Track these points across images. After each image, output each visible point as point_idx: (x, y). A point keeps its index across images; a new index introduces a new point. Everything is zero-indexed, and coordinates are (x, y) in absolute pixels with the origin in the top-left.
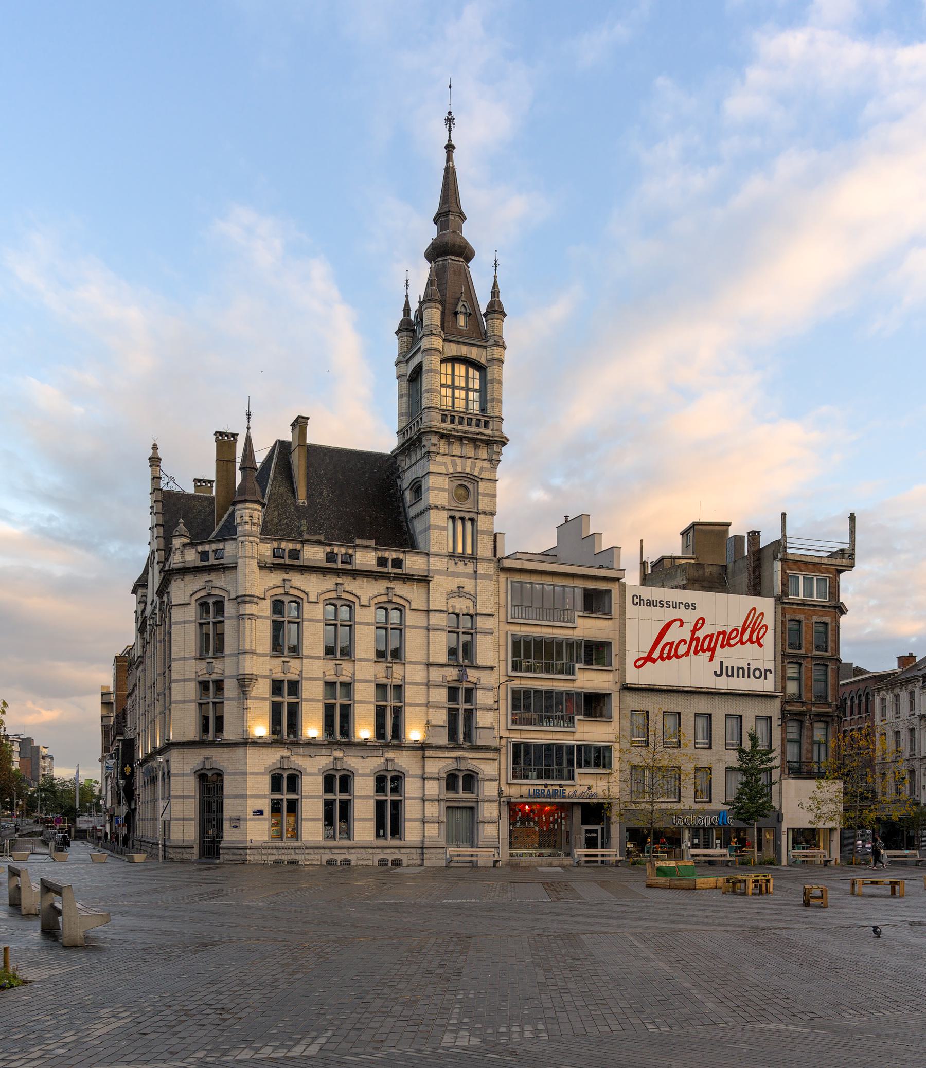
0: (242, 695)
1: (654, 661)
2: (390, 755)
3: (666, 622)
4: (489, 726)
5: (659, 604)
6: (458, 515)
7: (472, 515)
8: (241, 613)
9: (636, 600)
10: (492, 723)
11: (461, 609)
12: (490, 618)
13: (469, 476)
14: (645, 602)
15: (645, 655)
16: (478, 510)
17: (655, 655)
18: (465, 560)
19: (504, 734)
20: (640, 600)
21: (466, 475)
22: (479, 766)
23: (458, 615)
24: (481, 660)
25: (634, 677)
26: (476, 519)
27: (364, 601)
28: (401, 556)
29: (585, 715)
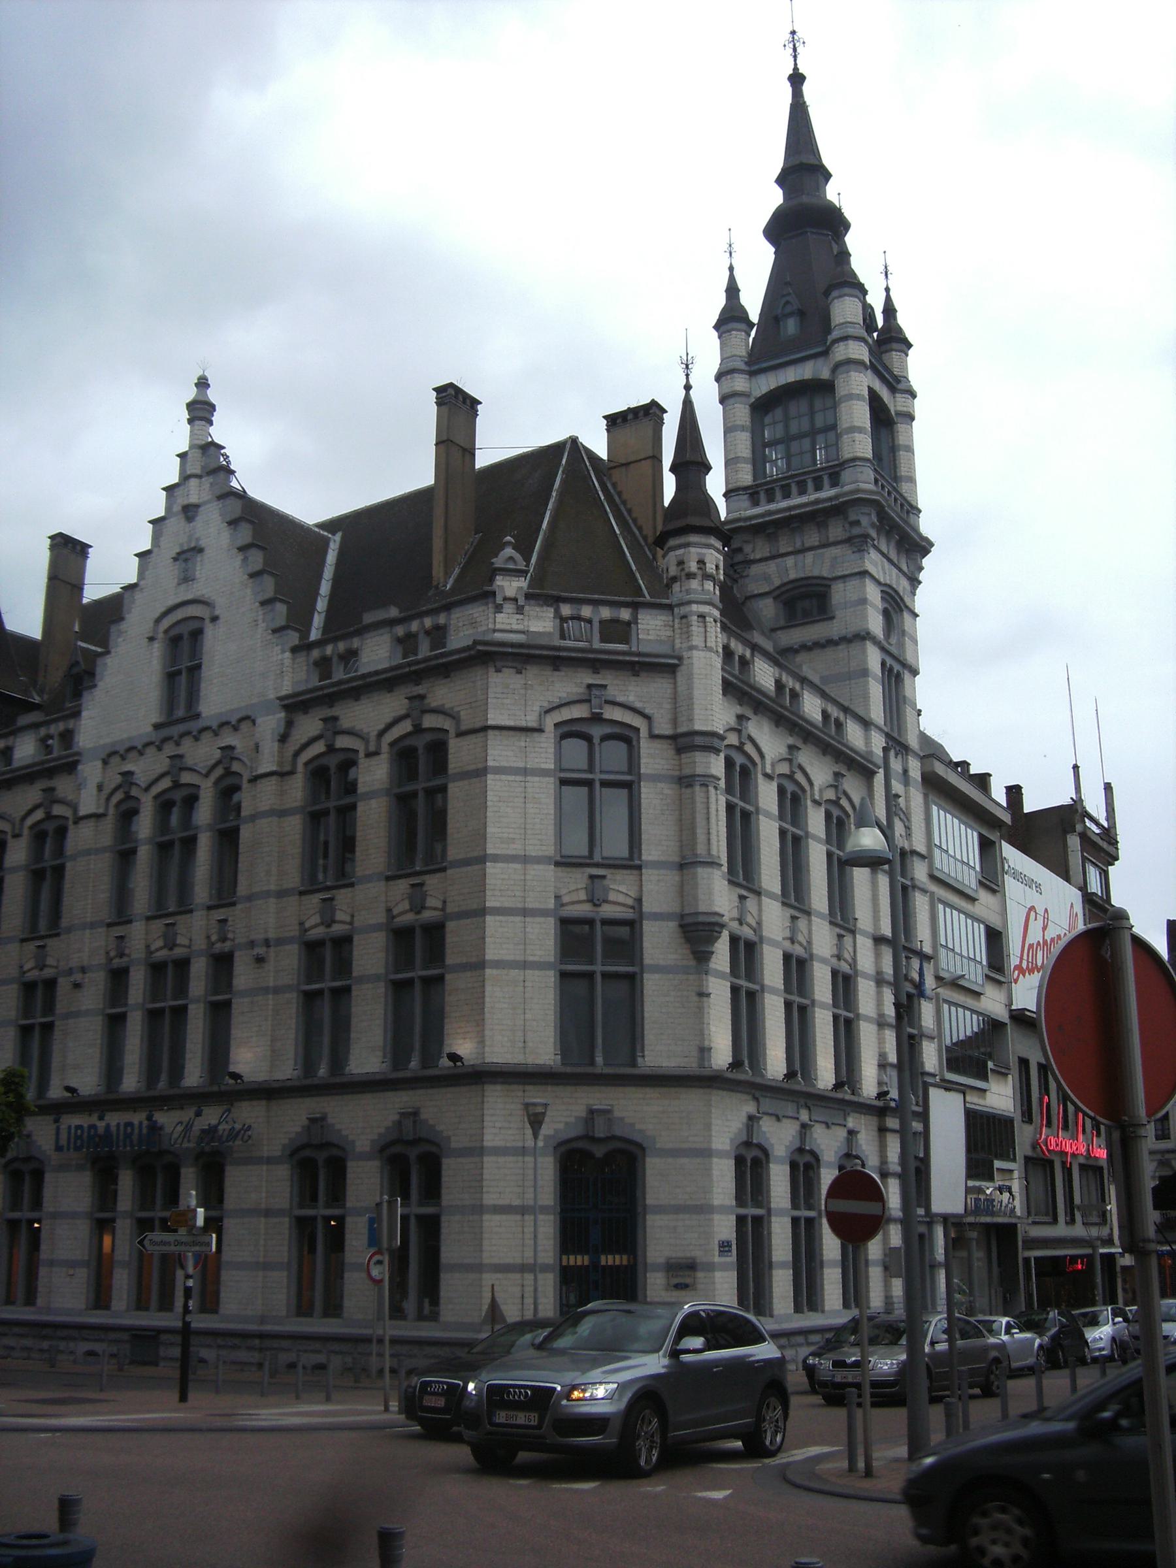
0: (693, 963)
8: (687, 771)
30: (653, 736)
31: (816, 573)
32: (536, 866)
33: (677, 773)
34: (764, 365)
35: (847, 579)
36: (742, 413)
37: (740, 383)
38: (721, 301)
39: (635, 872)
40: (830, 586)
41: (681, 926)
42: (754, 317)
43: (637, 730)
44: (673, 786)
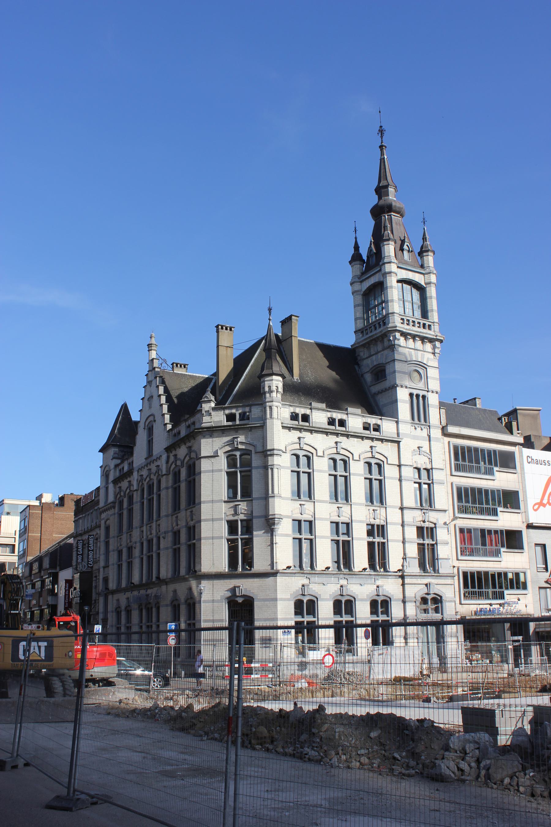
1: (544, 506)
2: (379, 582)
3: (549, 476)
4: (446, 557)
5: (543, 463)
6: (415, 392)
7: (425, 393)
9: (530, 460)
10: (448, 555)
11: (421, 464)
12: (441, 471)
13: (421, 364)
14: (535, 461)
15: (539, 501)
16: (428, 389)
17: (545, 501)
18: (422, 426)
19: (456, 563)
20: (532, 459)
21: (418, 363)
22: (441, 590)
23: (419, 470)
24: (438, 505)
25: (534, 519)
26: (427, 396)
27: (356, 457)
28: (379, 422)
29: (507, 548)
30: (256, 453)
31: (381, 362)
32: (217, 504)
33: (263, 465)
34: (364, 278)
35: (390, 363)
36: (359, 299)
37: (357, 287)
38: (352, 251)
39: (251, 502)
40: (385, 366)
41: (266, 520)
42: (365, 258)
43: (251, 451)
44: (264, 469)
